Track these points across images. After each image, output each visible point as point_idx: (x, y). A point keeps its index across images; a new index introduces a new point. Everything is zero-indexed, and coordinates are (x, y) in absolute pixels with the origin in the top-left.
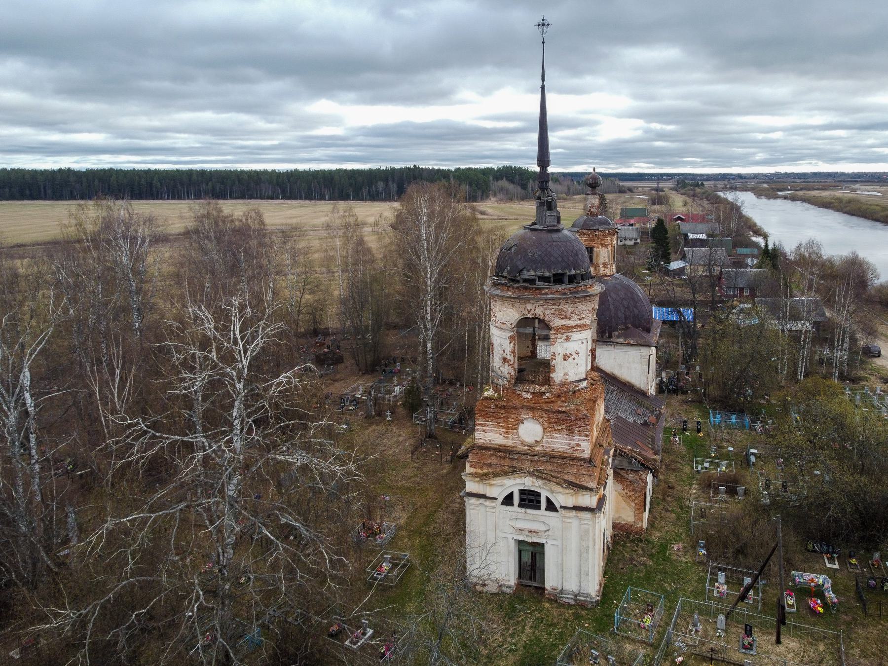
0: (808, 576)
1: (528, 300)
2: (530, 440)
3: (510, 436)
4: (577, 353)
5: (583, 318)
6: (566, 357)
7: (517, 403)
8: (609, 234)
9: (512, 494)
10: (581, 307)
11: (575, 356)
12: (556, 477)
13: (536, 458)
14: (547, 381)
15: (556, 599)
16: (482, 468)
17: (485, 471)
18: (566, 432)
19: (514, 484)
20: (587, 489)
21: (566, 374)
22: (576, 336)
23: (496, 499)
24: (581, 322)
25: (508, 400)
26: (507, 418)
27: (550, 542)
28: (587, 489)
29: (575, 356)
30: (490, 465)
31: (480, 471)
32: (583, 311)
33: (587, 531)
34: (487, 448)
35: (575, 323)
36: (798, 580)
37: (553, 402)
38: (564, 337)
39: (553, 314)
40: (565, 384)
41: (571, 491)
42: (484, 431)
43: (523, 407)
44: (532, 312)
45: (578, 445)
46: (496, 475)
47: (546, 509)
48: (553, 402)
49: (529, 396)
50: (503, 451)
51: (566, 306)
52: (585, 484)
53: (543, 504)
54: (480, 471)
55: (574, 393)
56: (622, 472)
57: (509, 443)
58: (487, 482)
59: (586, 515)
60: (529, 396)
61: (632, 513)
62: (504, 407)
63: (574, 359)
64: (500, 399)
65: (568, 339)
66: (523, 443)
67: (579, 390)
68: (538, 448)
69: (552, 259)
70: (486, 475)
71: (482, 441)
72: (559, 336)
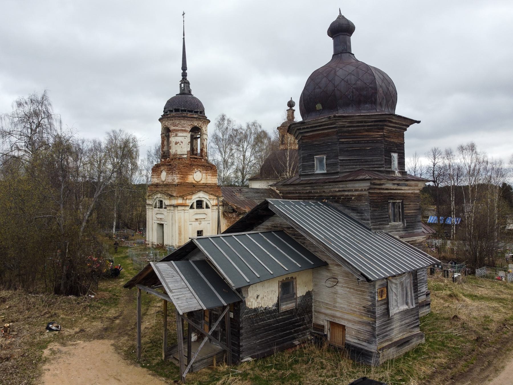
2: (163, 179)
4: (182, 142)
5: (184, 127)
6: (176, 143)
10: (183, 122)
11: (181, 144)
21: (176, 151)
22: (180, 134)
32: (184, 124)
35: (180, 129)
37: (170, 162)
38: (175, 134)
40: (176, 155)
51: (176, 121)
55: (179, 159)
63: (180, 144)
65: (176, 135)
67: (181, 158)
72: (173, 133)
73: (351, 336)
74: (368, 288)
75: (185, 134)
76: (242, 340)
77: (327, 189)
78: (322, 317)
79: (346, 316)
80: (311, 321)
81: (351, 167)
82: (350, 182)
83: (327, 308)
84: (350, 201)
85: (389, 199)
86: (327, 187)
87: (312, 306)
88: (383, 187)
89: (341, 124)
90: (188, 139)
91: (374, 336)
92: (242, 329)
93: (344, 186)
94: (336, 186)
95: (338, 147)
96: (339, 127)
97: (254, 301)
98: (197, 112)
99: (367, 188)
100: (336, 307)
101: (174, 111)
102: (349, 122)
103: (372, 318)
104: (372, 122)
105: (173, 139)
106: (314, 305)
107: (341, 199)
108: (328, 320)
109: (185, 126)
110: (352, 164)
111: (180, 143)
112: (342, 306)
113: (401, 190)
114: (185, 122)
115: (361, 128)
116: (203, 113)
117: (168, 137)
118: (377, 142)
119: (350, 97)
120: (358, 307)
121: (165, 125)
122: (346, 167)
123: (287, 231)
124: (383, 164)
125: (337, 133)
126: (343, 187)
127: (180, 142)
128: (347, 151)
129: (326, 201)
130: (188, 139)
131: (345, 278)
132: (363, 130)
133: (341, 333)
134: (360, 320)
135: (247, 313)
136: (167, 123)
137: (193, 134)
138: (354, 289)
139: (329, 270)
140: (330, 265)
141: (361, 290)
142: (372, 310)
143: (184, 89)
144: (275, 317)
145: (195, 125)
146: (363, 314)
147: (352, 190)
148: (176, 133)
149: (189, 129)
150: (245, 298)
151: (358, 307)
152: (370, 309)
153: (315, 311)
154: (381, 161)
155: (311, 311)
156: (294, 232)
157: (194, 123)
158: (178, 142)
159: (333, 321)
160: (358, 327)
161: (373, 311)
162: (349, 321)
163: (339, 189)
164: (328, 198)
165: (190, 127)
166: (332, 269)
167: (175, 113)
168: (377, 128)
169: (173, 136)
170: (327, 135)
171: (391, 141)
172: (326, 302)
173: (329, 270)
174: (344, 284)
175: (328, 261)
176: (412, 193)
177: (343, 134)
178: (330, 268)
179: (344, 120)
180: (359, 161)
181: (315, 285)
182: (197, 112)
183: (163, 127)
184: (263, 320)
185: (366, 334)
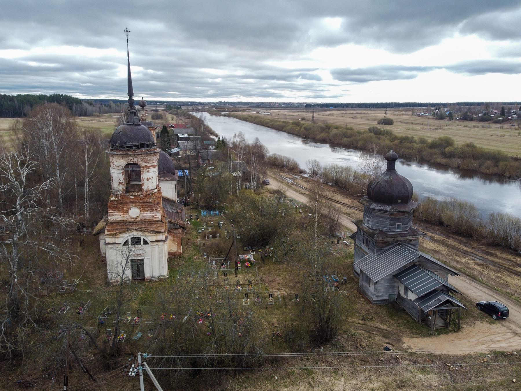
0: (244, 256)
1: (130, 155)
2: (134, 216)
3: (125, 216)
4: (152, 178)
6: (148, 179)
7: (127, 201)
8: (152, 129)
9: (128, 240)
10: (153, 157)
11: (151, 179)
12: (148, 230)
13: (138, 223)
14: (141, 190)
15: (150, 280)
16: (113, 231)
17: (115, 232)
18: (150, 210)
19: (127, 236)
20: (161, 232)
21: (148, 187)
22: (152, 170)
23: (121, 243)
24: (153, 164)
25: (123, 200)
26: (123, 208)
27: (146, 258)
28: (161, 232)
29: (151, 179)
30: (117, 229)
31: (112, 233)
33: (162, 250)
34: (114, 223)
35: (151, 165)
36: (241, 258)
37: (143, 199)
38: (147, 171)
39: (142, 161)
41: (154, 234)
42: (112, 215)
43: (131, 202)
44: (132, 161)
45: (156, 215)
46: (120, 233)
47: (144, 244)
48: (143, 199)
49: (133, 197)
50: (122, 223)
52: (160, 231)
53: (142, 242)
54: (112, 233)
55: (152, 194)
56: (171, 230)
57: (125, 219)
58: (116, 236)
59: (161, 243)
60: (133, 197)
61: (176, 247)
62: (121, 203)
64: (119, 200)
65: (148, 171)
66: (131, 218)
67: (154, 193)
68: (139, 219)
69: (139, 137)
70: (115, 234)
71: (112, 220)
72: (145, 170)
127: (151, 178)
158: (150, 178)
169: (144, 172)
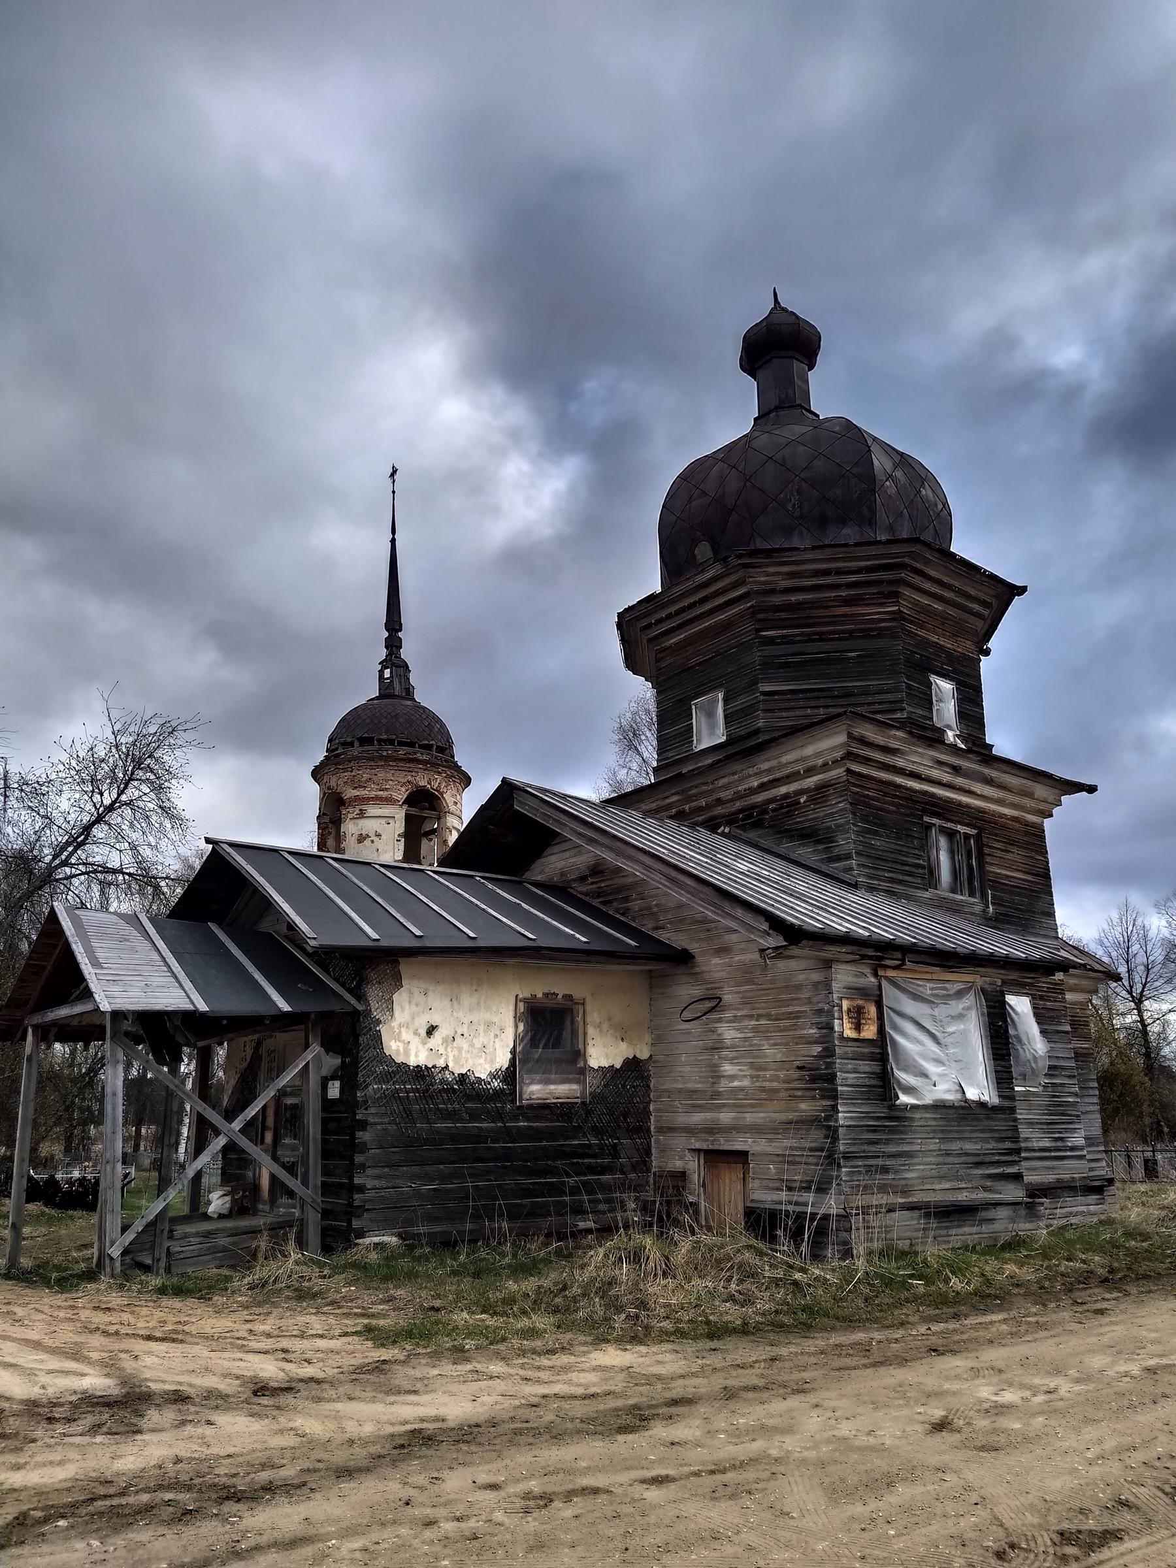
4: (378, 835)
6: (361, 839)
10: (381, 775)
11: (374, 838)
22: (373, 810)
32: (387, 781)
63: (372, 842)
65: (362, 815)
72: (350, 810)
73: (765, 1183)
74: (809, 1001)
75: (387, 810)
76: (363, 1167)
77: (726, 787)
78: (680, 1142)
79: (749, 1118)
80: (643, 1164)
81: (798, 713)
82: (783, 740)
83: (695, 1106)
84: (796, 810)
85: (925, 812)
86: (725, 781)
87: (648, 1113)
88: (900, 762)
89: (766, 583)
90: (399, 826)
91: (832, 1159)
92: (364, 1129)
93: (773, 763)
94: (751, 771)
95: (756, 656)
96: (757, 593)
97: (415, 1042)
98: (428, 747)
99: (839, 754)
100: (716, 1095)
101: (356, 744)
102: (787, 574)
103: (823, 1097)
104: (859, 571)
105: (350, 828)
106: (654, 1109)
107: (767, 813)
108: (699, 1151)
109: (388, 787)
110: (802, 703)
111: (374, 838)
112: (736, 1084)
113: (970, 793)
114: (389, 776)
115: (827, 595)
116: (448, 751)
117: (337, 822)
118: (879, 636)
119: (794, 505)
120: (782, 1074)
121: (329, 788)
122: (784, 714)
123: (580, 889)
124: (901, 701)
125: (754, 611)
126: (769, 771)
128: (787, 665)
129: (727, 830)
130: (398, 825)
131: (742, 989)
132: (837, 599)
133: (739, 1186)
134: (791, 1116)
135: (387, 1077)
136: (334, 779)
137: (413, 811)
138: (768, 1016)
139: (696, 976)
140: (699, 959)
141: (791, 1013)
142: (826, 1069)
143: (392, 681)
144: (500, 1115)
145: (422, 783)
146: (799, 1093)
147: (799, 772)
148: (362, 807)
149: (401, 795)
150: (378, 1022)
151: (782, 1074)
152: (818, 1069)
153: (660, 1130)
154: (897, 690)
155: (641, 1130)
156: (598, 885)
157: (417, 778)
159: (711, 1147)
160: (788, 1143)
161: (828, 1074)
162: (756, 1130)
163: (760, 781)
164: (731, 820)
165: (403, 789)
166: (704, 969)
167: (361, 749)
168: (879, 593)
169: (350, 816)
170: (727, 625)
171: (928, 639)
172: (690, 1086)
173: (696, 976)
174: (739, 1009)
175: (694, 948)
176: (1015, 819)
177: (770, 615)
178: (697, 970)
179: (771, 570)
180: (825, 694)
181: (657, 1041)
182: (428, 747)
183: (325, 794)
184: (451, 1116)
185: (811, 1160)
